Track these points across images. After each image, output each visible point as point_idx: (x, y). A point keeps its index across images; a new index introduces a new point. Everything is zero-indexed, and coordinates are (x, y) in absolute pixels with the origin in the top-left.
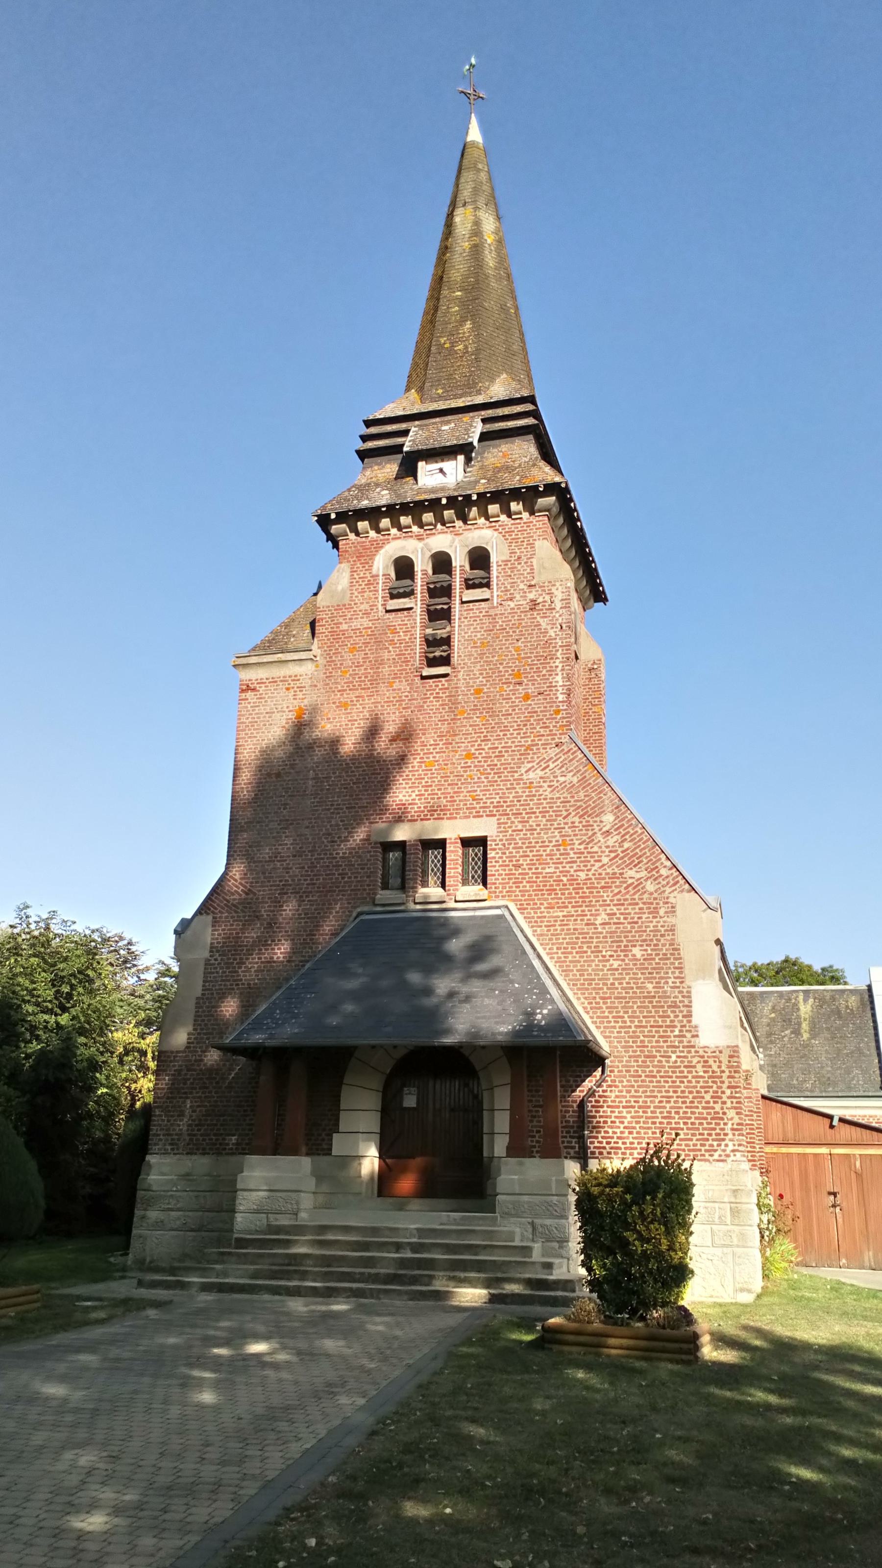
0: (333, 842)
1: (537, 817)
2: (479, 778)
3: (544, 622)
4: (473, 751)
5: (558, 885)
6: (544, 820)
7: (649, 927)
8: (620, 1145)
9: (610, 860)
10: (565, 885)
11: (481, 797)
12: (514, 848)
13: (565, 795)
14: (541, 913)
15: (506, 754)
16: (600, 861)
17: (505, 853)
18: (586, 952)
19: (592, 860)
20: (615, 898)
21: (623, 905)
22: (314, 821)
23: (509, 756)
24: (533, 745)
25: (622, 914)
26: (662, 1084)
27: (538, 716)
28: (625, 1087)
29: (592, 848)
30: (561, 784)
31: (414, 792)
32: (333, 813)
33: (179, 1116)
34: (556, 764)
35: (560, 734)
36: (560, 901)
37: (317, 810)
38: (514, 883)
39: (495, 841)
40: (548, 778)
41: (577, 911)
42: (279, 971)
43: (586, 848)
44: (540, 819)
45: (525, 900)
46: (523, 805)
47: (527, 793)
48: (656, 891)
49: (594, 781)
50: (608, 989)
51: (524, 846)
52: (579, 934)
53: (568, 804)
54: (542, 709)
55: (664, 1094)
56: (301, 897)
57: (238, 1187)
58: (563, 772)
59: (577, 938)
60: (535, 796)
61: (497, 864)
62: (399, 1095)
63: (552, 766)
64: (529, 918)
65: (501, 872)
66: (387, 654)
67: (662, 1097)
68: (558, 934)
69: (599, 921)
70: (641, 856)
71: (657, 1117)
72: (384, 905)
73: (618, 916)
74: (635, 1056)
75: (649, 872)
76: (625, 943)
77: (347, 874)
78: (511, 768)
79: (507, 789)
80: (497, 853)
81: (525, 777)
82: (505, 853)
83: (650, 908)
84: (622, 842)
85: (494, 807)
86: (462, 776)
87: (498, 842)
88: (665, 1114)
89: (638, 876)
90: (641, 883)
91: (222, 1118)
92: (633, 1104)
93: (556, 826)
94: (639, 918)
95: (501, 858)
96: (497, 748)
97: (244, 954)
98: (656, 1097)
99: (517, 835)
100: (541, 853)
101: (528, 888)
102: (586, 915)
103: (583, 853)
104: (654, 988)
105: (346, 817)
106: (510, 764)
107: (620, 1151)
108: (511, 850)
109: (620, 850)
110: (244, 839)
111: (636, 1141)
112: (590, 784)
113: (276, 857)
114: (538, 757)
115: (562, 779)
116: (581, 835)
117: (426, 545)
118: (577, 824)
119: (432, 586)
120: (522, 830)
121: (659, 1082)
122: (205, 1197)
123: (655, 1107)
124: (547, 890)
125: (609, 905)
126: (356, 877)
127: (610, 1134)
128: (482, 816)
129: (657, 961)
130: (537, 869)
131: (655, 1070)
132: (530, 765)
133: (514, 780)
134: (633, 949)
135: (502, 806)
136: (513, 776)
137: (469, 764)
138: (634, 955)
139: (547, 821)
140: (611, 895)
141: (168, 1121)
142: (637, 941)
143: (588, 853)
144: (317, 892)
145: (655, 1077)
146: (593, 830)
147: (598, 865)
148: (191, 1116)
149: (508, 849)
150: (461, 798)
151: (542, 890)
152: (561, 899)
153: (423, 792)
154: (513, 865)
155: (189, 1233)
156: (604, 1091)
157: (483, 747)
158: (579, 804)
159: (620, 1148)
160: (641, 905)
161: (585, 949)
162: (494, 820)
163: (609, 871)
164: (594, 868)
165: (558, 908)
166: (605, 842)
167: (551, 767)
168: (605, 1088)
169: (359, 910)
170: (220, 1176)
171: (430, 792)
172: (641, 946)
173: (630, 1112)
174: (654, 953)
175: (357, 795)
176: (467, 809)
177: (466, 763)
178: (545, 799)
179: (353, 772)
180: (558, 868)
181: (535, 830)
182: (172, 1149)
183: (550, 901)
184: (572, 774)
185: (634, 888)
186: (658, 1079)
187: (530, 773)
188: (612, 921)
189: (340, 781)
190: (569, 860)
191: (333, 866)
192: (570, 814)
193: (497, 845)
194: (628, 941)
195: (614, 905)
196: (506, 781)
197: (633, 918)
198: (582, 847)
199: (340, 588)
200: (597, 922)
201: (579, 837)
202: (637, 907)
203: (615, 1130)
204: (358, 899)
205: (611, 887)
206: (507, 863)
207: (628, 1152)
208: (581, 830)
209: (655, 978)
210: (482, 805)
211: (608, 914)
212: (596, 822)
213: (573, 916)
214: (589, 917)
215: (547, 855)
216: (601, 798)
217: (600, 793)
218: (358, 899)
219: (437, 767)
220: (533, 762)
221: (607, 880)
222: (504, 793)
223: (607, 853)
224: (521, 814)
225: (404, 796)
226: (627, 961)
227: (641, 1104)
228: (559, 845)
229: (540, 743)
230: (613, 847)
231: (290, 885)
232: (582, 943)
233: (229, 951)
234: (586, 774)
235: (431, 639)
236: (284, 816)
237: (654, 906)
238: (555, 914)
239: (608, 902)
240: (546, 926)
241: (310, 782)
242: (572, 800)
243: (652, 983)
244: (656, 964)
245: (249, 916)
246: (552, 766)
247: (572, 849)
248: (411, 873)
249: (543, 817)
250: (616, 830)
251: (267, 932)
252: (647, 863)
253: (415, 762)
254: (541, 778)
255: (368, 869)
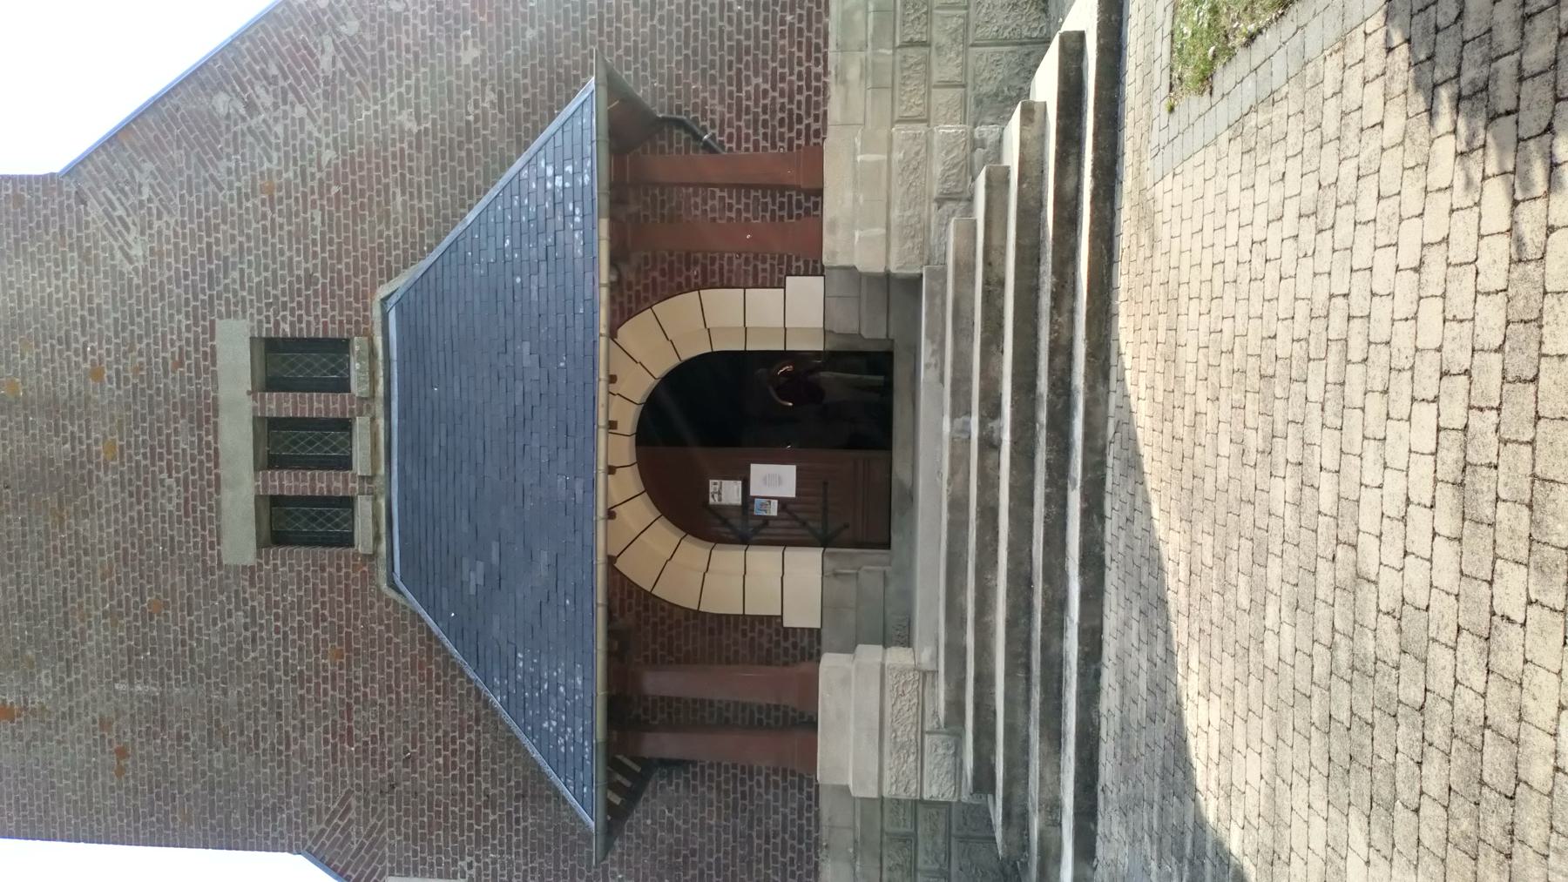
0: (254, 640)
1: (217, 240)
2: (140, 354)
4: (88, 366)
5: (346, 201)
6: (222, 227)
7: (423, 32)
8: (802, 98)
9: (301, 102)
10: (345, 191)
11: (176, 349)
12: (275, 287)
13: (177, 186)
14: (396, 237)
15: (96, 301)
16: (302, 120)
17: (284, 304)
18: (469, 152)
19: (300, 136)
20: (371, 94)
21: (383, 81)
22: (213, 680)
23: (98, 295)
24: (80, 247)
25: (400, 82)
26: (699, 17)
27: (24, 239)
28: (704, 85)
29: (277, 137)
30: (157, 195)
31: (162, 481)
32: (199, 641)
34: (117, 204)
35: (60, 194)
36: (376, 199)
37: (192, 671)
38: (341, 287)
39: (260, 322)
40: (142, 218)
41: (394, 167)
42: (495, 739)
43: (278, 149)
44: (220, 236)
45: (373, 266)
46: (194, 269)
47: (172, 260)
48: (359, 17)
49: (151, 130)
50: (534, 113)
51: (272, 267)
52: (435, 164)
53: (194, 181)
54: (11, 229)
55: (717, 14)
56: (357, 700)
58: (132, 189)
59: (444, 169)
60: (176, 245)
61: (305, 318)
62: (720, 513)
63: (120, 212)
64: (405, 259)
65: (319, 312)
67: (722, 19)
68: (437, 205)
69: (412, 126)
70: (295, 44)
71: (756, 28)
73: (403, 90)
74: (653, 66)
75: (324, 29)
76: (453, 78)
77: (316, 610)
78: (122, 291)
79: (162, 297)
80: (284, 318)
81: (140, 264)
82: (284, 304)
83: (389, 30)
84: (266, 78)
85: (196, 324)
86: (135, 386)
87: (262, 317)
88: (751, 13)
89: (330, 49)
90: (343, 43)
91: (756, 841)
92: (733, 73)
93: (235, 205)
94: (408, 51)
95: (292, 310)
96: (82, 318)
97: (462, 810)
98: (721, 30)
99: (250, 280)
100: (284, 233)
101: (351, 261)
102: (402, 150)
103: (286, 153)
104: (532, 26)
105: (207, 613)
106: (114, 292)
107: (814, 99)
108: (278, 292)
109: (282, 83)
110: (243, 819)
111: (797, 69)
112: (156, 137)
113: (280, 753)
114: (104, 239)
115: (146, 192)
116: (253, 156)
118: (233, 165)
120: (242, 271)
121: (696, 21)
122: (890, 869)
123: (739, 33)
124: (355, 223)
125: (384, 106)
126: (323, 594)
127: (785, 115)
128: (213, 347)
129: (484, 19)
130: (314, 242)
131: (676, 30)
132: (119, 255)
133: (145, 284)
134: (463, 62)
135: (195, 308)
136: (138, 287)
137: (113, 373)
138: (475, 61)
139: (225, 222)
140: (364, 101)
142: (449, 54)
143: (286, 143)
144: (349, 669)
145: (687, 29)
146: (243, 134)
147: (309, 126)
149: (276, 297)
150: (177, 388)
151: (355, 232)
152: (370, 198)
153: (164, 464)
154: (307, 289)
156: (713, 126)
157: (80, 346)
158: (193, 160)
159: (808, 98)
160: (385, 45)
161: (463, 154)
162: (220, 325)
163: (320, 106)
164: (316, 134)
165: (387, 203)
166: (266, 109)
167: (124, 214)
168: (708, 124)
169: (384, 586)
170: (855, 841)
171: (164, 451)
172: (458, 47)
173: (748, 77)
174: (471, 24)
175: (166, 595)
176: (198, 377)
177: (109, 378)
178: (184, 226)
179: (120, 605)
180: (314, 202)
181: (241, 244)
183: (375, 218)
184: (136, 172)
185: (353, 58)
186: (691, 24)
187: (132, 253)
188: (413, 101)
189: (137, 628)
190: (299, 180)
191: (300, 638)
192: (211, 176)
193: (268, 318)
194: (449, 72)
195: (384, 95)
196: (146, 301)
197: (408, 61)
198: (275, 155)
200: (415, 130)
201: (256, 161)
202: (387, 54)
203: (778, 106)
204: (364, 589)
205: (351, 101)
206: (302, 299)
207: (814, 84)
208: (243, 155)
209: (515, 23)
210: (191, 349)
211: (401, 108)
212: (228, 128)
213: (402, 175)
214: (405, 145)
215: (290, 223)
216: (183, 116)
217: (173, 118)
218: (364, 589)
219: (116, 437)
220: (112, 248)
221: (338, 108)
222: (171, 305)
223: (288, 107)
224: (210, 271)
225: (170, 500)
226: (486, 75)
227: (733, 58)
228: (271, 198)
229: (75, 234)
230: (275, 96)
231: (334, 722)
232: (452, 159)
233: (455, 841)
234: (138, 145)
236: (202, 739)
237: (385, 20)
238: (400, 209)
239: (378, 108)
240: (421, 228)
241: (139, 688)
242: (186, 172)
243: (524, 29)
244: (490, 19)
245: (391, 803)
246: (120, 212)
247: (279, 173)
248: (318, 485)
249: (217, 231)
250: (245, 91)
251: (422, 765)
252: (308, 32)
253: (104, 479)
254: (142, 233)
255: (307, 569)
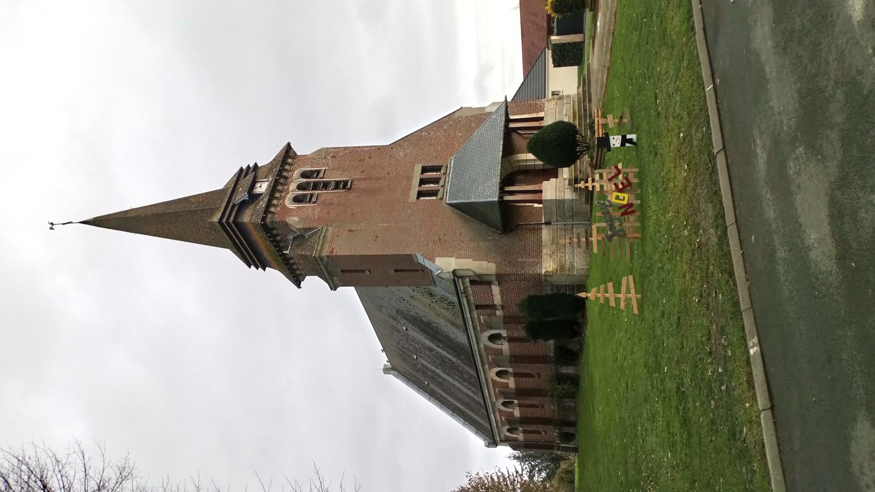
3: (341, 154)
33: (525, 263)
57: (555, 198)
66: (335, 202)
72: (443, 196)
115: (406, 146)
117: (292, 191)
119: (311, 189)
132: (398, 156)
141: (527, 267)
147: (440, 136)
148: (525, 258)
155: (575, 251)
182: (539, 264)
199: (297, 220)
235: (334, 187)
246: (400, 149)
